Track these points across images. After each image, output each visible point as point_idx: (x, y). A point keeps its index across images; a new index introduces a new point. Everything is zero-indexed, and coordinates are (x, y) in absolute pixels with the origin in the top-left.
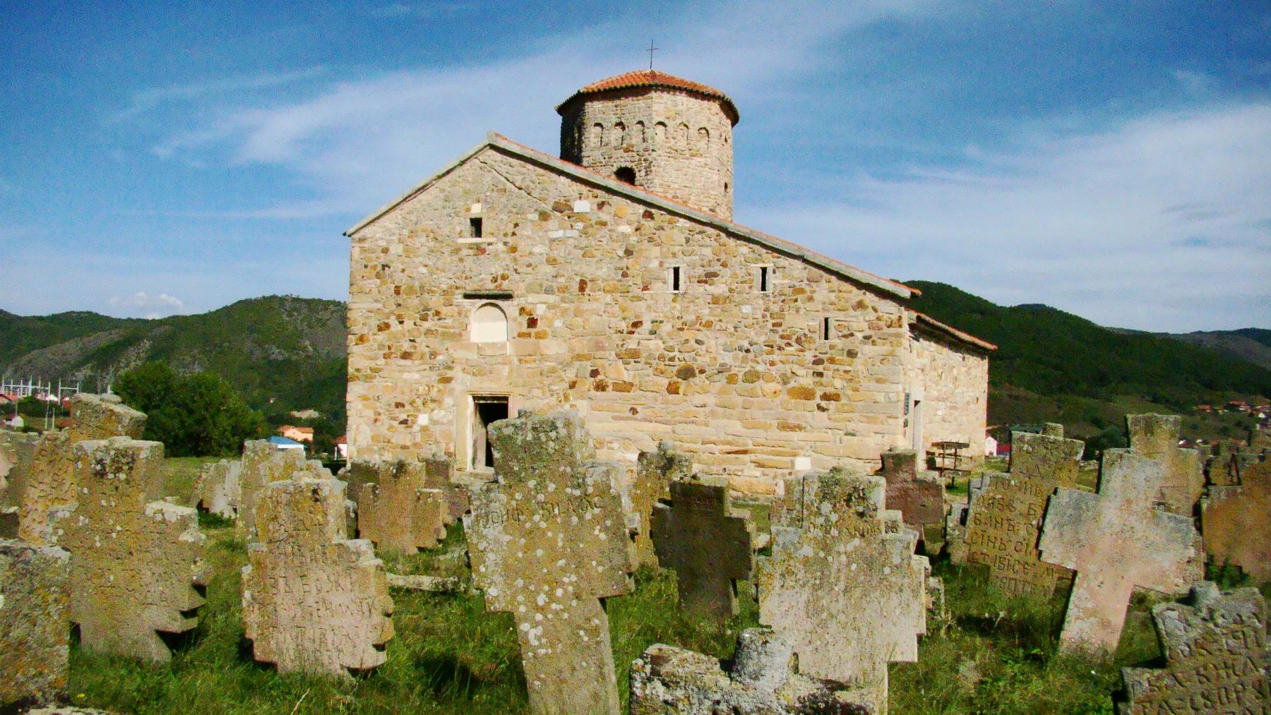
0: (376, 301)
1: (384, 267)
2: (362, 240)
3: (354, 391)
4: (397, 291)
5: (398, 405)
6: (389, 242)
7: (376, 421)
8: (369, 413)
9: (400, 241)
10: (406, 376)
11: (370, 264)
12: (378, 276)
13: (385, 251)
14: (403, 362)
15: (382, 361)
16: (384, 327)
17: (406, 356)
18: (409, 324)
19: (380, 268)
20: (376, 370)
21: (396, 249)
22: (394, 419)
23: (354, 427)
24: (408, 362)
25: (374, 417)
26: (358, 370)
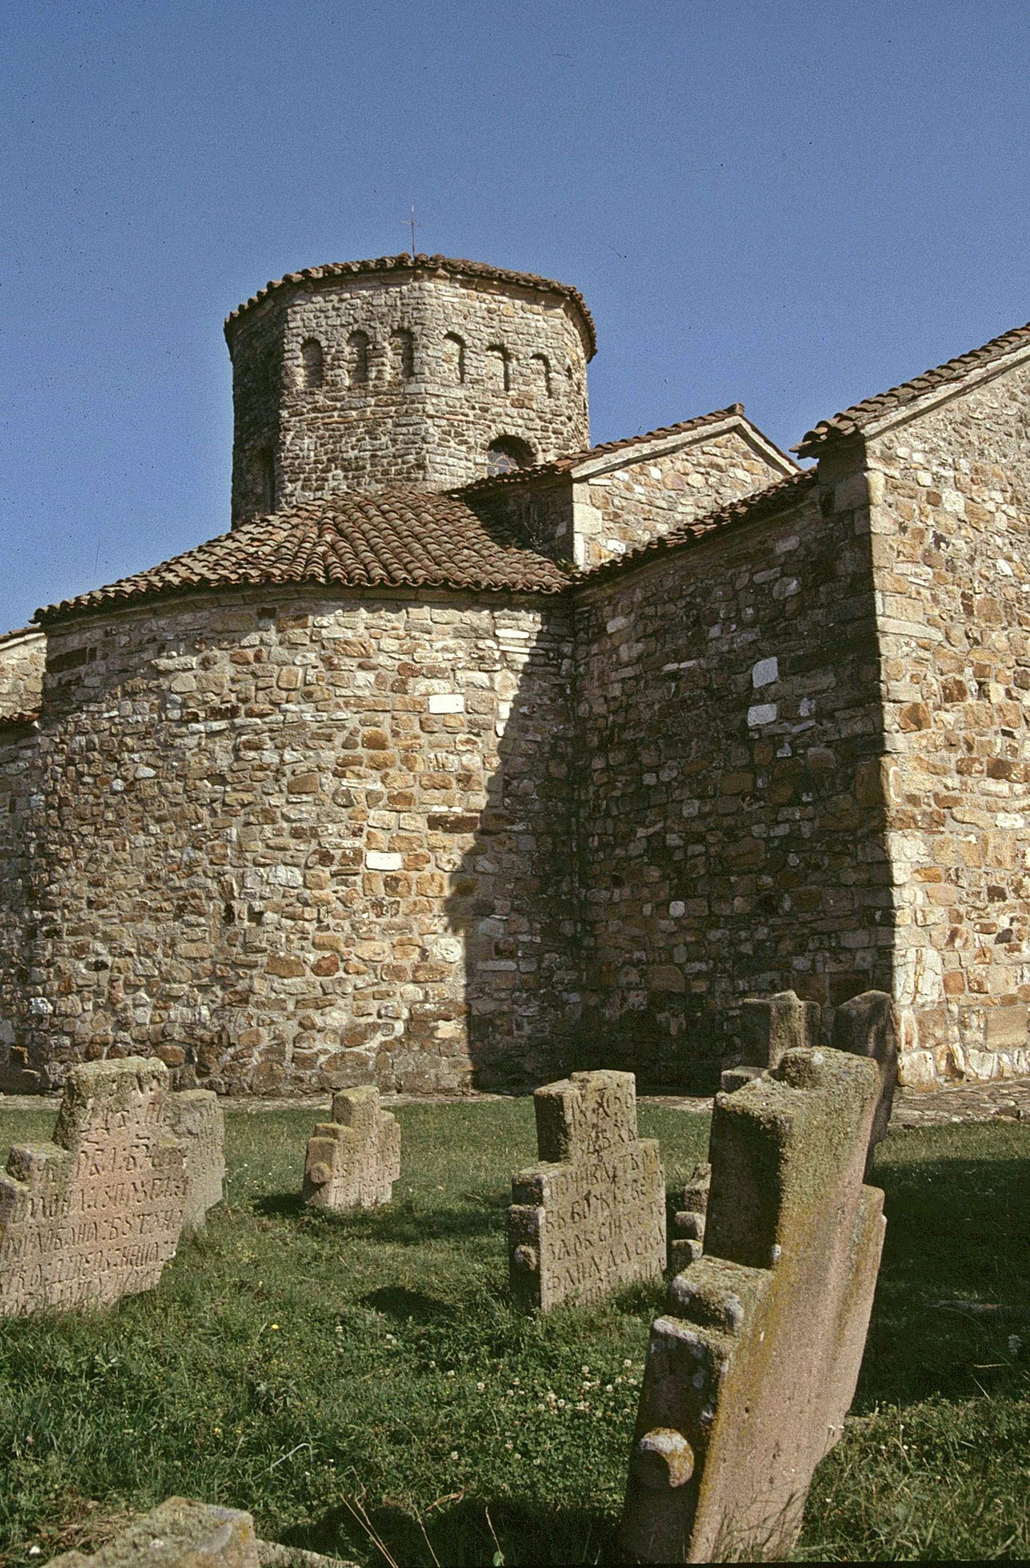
0: (931, 622)
1: (939, 539)
2: (888, 459)
3: (906, 851)
4: (969, 610)
5: (996, 893)
6: (937, 478)
7: (954, 934)
8: (938, 914)
9: (958, 486)
10: (1003, 820)
11: (910, 525)
12: (928, 560)
13: (935, 500)
14: (992, 785)
15: (953, 781)
16: (953, 693)
17: (999, 770)
18: (997, 691)
19: (929, 538)
20: (947, 803)
21: (953, 501)
22: (986, 930)
23: (911, 956)
24: (1002, 787)
25: (946, 927)
26: (913, 799)
